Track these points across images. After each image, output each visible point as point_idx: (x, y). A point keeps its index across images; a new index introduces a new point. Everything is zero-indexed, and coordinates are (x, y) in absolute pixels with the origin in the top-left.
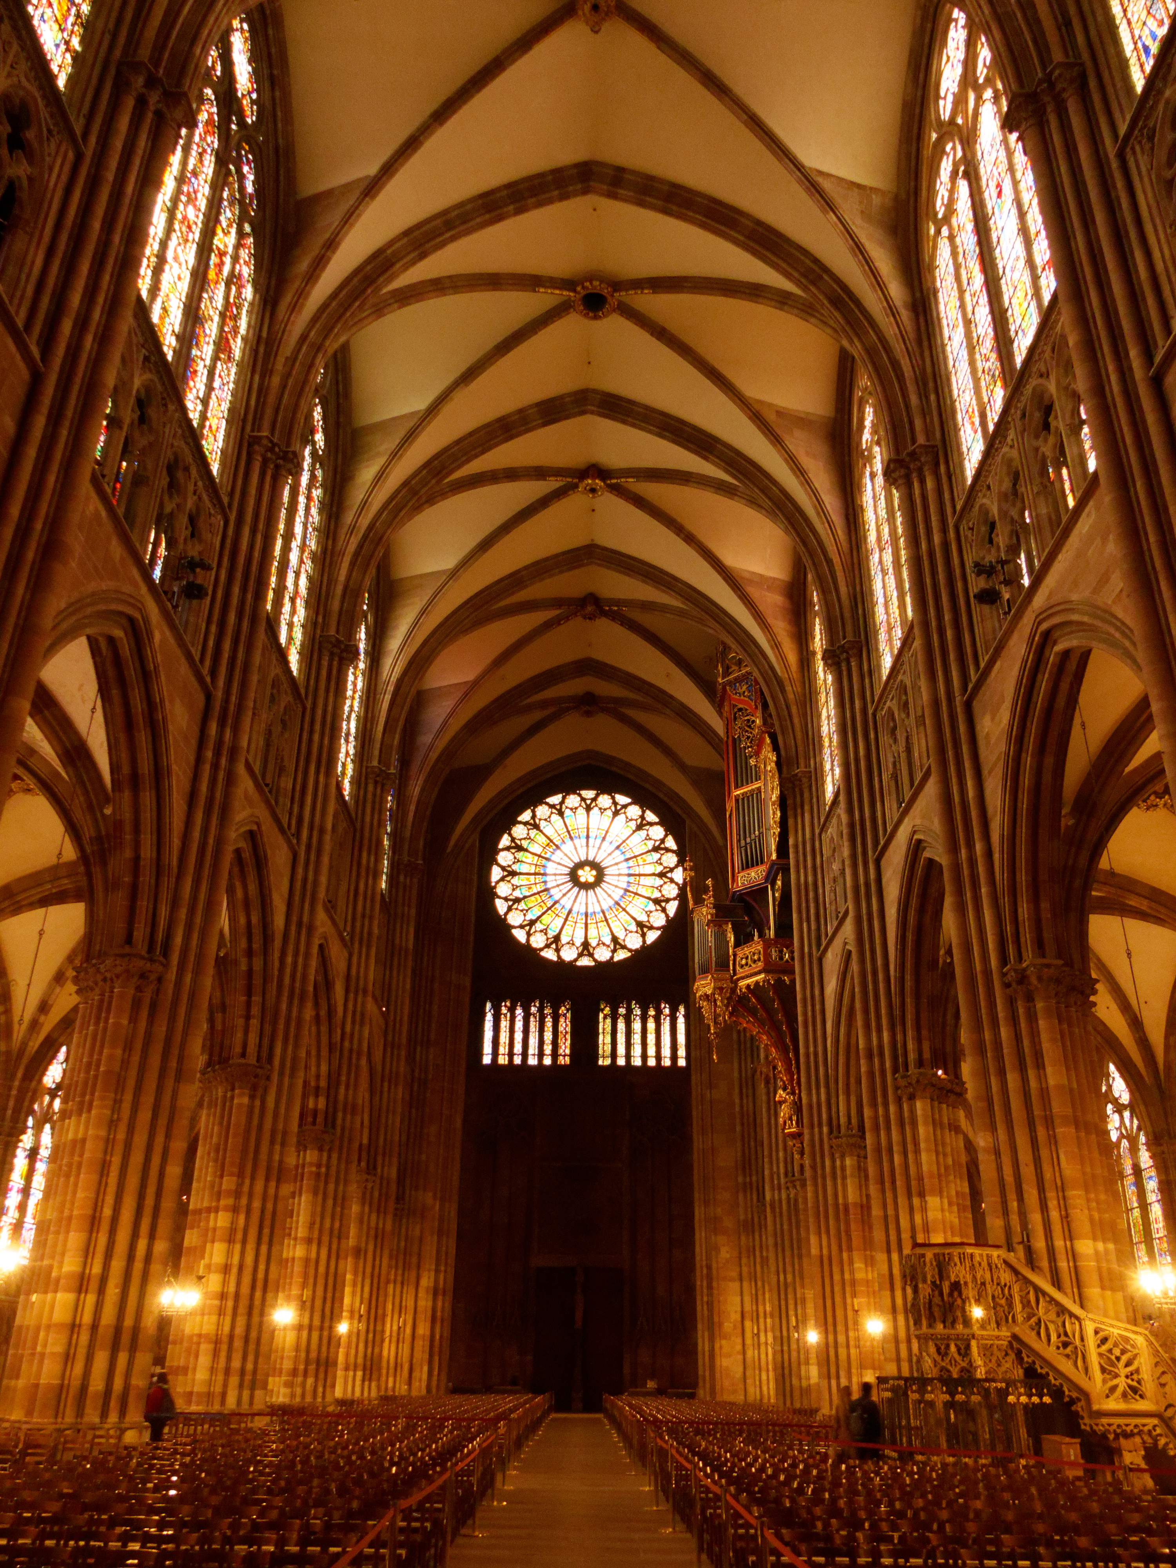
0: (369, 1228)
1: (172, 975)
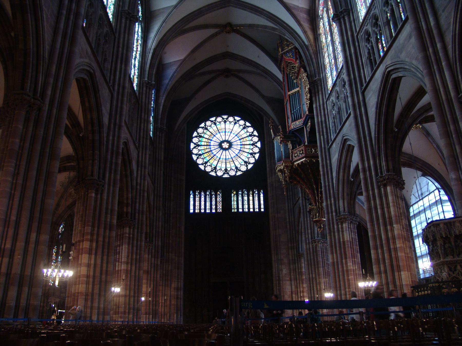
0: (151, 263)
1: (46, 108)
